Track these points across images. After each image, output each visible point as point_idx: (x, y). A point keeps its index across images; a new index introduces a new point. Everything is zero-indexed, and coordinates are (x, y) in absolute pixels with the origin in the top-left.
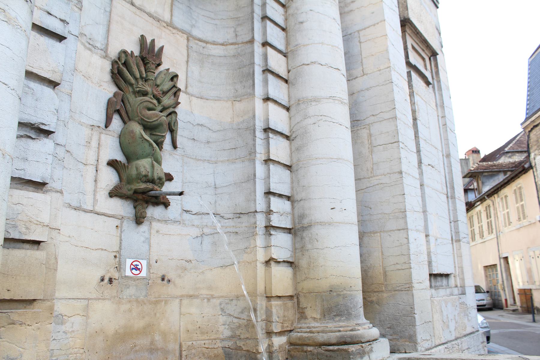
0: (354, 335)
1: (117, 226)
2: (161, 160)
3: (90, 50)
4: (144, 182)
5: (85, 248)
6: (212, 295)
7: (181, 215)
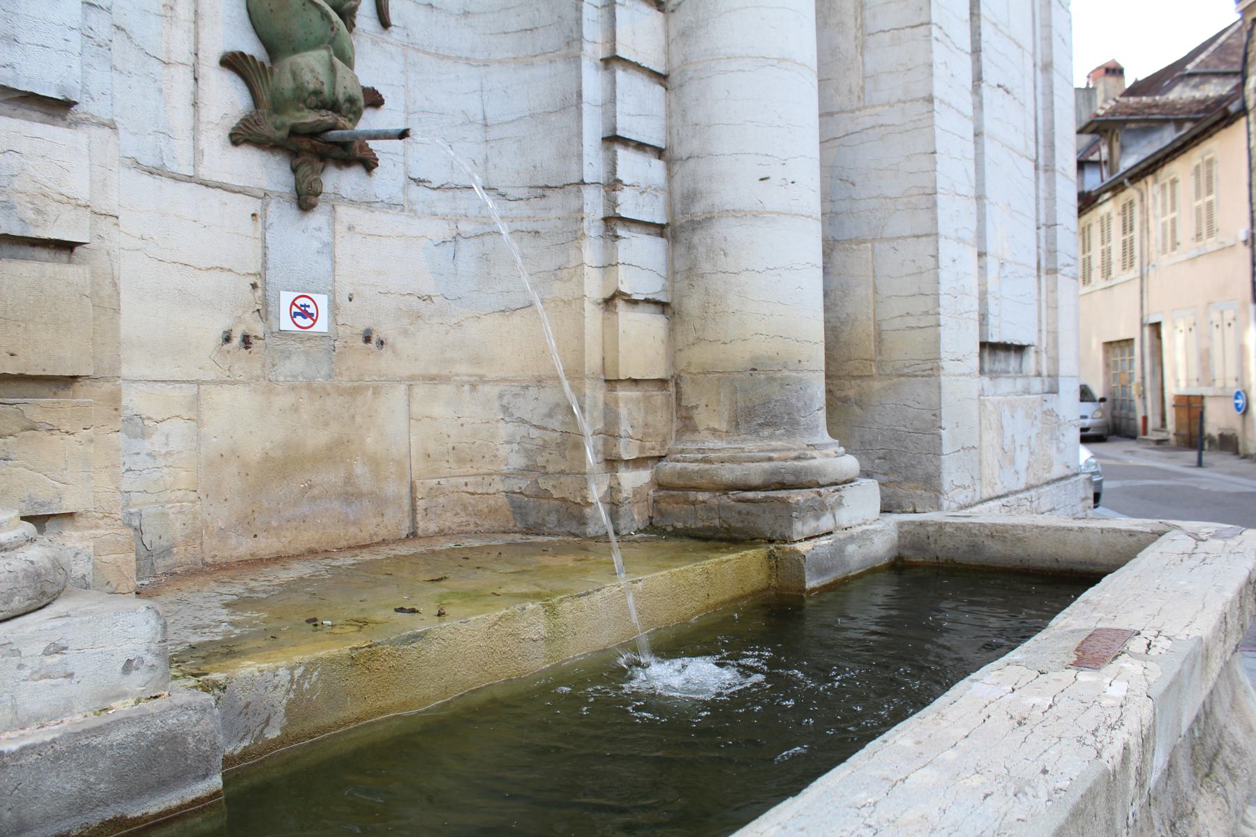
0: (802, 468)
1: (254, 215)
2: (351, 54)
4: (312, 109)
5: (183, 267)
6: (481, 377)
7: (404, 189)
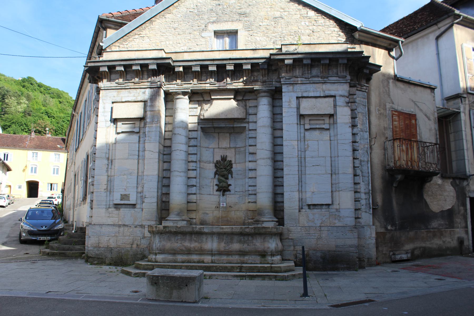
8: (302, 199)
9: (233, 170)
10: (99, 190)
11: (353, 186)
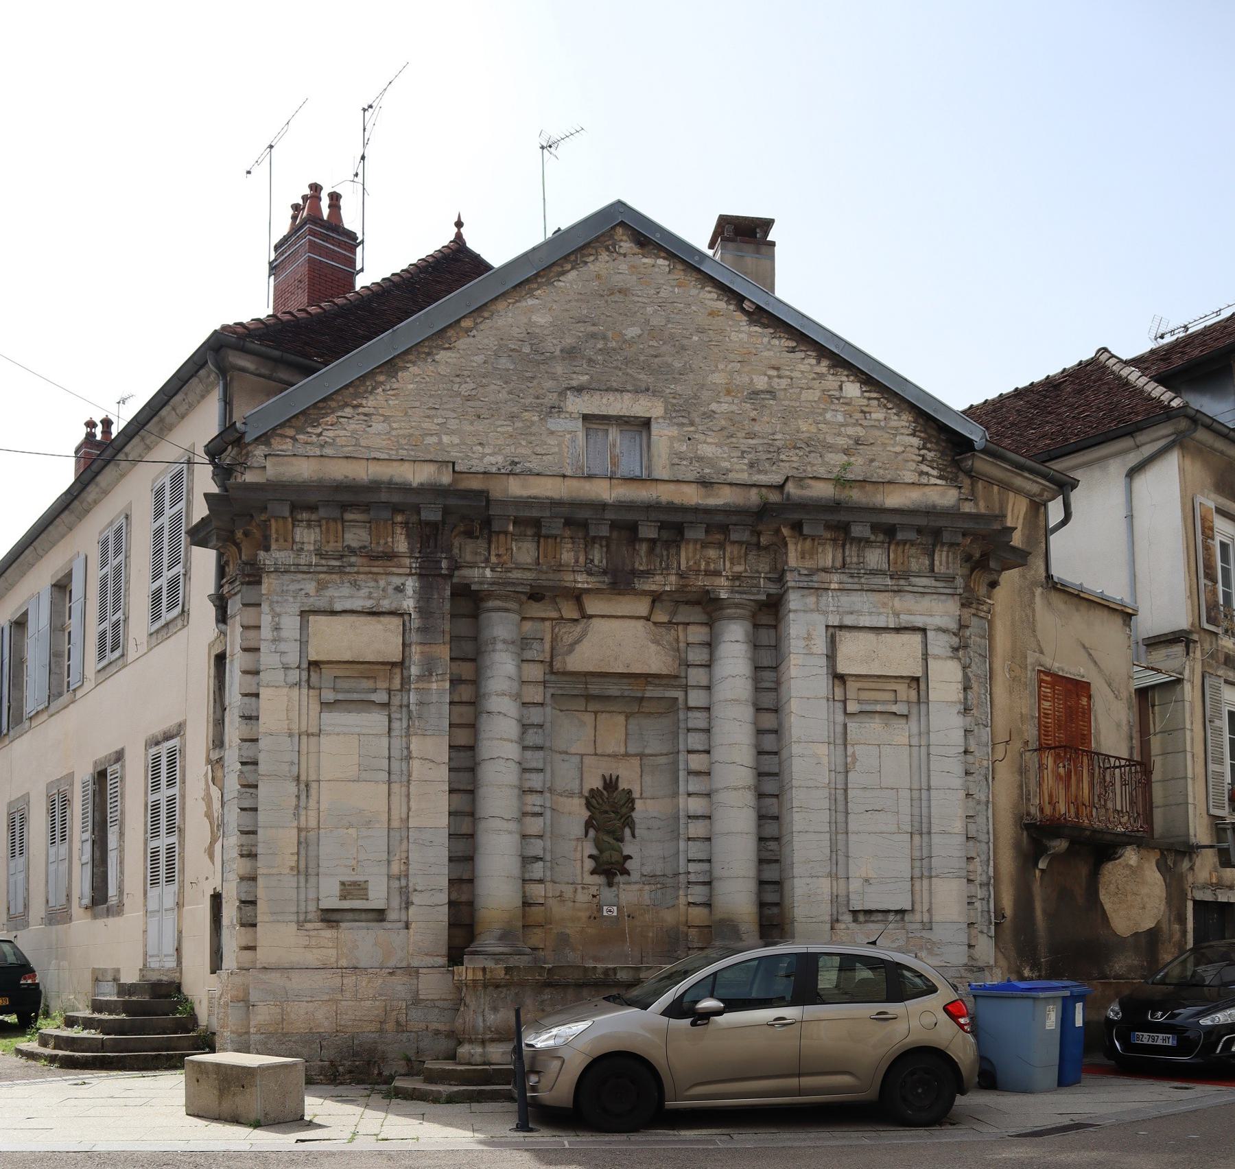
3: (572, 797)
8: (837, 896)
9: (636, 815)
10: (274, 871)
11: (963, 865)
